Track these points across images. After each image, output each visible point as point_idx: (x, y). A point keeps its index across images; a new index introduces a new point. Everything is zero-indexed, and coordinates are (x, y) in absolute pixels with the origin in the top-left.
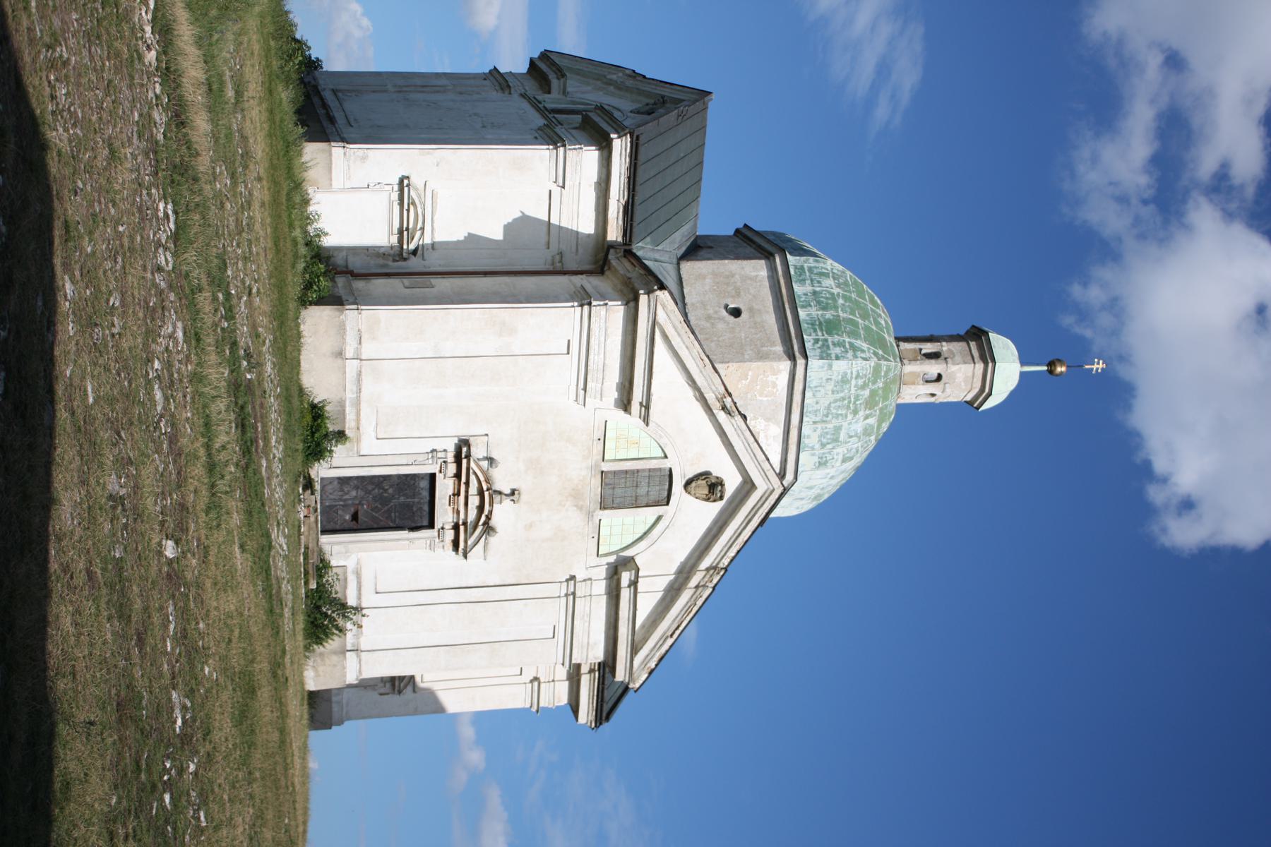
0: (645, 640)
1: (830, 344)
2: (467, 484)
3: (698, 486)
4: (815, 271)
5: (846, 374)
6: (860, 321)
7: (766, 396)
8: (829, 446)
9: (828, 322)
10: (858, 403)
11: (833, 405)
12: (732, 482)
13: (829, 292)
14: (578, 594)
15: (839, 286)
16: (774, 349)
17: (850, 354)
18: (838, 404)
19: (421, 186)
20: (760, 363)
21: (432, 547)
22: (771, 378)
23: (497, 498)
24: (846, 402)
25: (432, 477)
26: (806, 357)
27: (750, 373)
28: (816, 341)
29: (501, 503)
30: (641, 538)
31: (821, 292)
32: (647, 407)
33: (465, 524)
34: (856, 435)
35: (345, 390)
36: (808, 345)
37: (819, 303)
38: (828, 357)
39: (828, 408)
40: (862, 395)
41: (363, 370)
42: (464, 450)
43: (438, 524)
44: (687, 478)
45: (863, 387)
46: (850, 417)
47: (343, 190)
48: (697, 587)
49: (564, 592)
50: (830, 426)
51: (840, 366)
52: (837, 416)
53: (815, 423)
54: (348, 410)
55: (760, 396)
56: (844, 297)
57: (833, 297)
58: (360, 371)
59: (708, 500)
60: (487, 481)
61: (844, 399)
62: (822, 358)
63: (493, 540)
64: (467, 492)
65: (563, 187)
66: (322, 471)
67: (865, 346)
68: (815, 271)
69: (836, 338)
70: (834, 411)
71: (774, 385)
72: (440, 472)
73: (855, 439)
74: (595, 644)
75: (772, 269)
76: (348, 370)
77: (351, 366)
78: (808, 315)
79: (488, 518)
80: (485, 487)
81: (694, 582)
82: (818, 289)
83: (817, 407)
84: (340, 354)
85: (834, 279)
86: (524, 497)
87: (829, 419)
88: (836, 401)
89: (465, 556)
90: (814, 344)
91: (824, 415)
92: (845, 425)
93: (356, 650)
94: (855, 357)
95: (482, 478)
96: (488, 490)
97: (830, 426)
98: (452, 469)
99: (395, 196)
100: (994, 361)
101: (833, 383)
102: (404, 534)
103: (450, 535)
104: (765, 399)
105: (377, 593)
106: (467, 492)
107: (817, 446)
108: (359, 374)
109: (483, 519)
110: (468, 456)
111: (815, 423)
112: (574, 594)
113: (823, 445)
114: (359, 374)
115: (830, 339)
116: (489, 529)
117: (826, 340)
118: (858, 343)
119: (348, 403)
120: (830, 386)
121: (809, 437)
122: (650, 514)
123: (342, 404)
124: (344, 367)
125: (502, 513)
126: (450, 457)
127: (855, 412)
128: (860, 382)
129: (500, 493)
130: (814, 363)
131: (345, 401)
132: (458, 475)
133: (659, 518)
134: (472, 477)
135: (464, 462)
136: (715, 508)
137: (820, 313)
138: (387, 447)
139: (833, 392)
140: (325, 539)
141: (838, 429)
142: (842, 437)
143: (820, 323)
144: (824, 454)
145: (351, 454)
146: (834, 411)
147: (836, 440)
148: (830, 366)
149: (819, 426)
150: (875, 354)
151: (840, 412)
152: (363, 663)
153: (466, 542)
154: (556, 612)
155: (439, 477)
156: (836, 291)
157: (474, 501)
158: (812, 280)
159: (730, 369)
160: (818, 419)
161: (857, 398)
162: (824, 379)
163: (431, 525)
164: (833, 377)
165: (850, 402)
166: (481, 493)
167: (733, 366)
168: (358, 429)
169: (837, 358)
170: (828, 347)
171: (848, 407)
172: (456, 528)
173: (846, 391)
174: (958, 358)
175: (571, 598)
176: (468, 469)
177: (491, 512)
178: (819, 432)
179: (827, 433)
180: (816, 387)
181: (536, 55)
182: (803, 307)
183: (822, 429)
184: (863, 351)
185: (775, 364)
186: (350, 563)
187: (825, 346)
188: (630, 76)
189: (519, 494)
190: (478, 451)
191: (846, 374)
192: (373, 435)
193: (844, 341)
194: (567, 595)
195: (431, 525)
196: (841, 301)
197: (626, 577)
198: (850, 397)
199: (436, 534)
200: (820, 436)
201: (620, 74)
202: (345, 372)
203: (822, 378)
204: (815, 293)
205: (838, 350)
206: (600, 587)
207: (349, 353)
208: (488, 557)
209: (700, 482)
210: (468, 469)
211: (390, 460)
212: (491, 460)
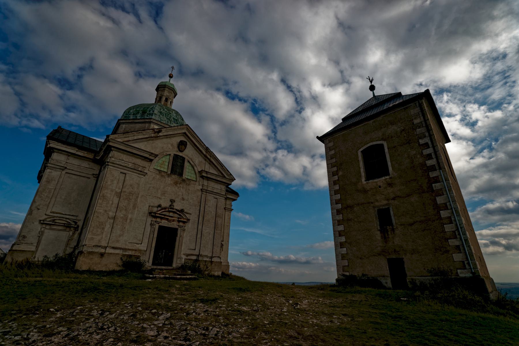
0: (222, 174)
2: (165, 215)
3: (181, 148)
4: (127, 113)
5: (159, 111)
8: (178, 122)
9: (143, 112)
12: (183, 139)
14: (206, 189)
16: (146, 127)
17: (153, 109)
19: (47, 217)
21: (184, 230)
23: (172, 207)
25: (159, 226)
26: (151, 119)
28: (147, 116)
29: (174, 206)
30: (194, 168)
32: (152, 154)
33: (178, 218)
35: (119, 254)
36: (148, 118)
37: (136, 114)
38: (152, 114)
39: (167, 119)
41: (112, 246)
42: (152, 214)
43: (177, 227)
44: (178, 150)
46: (171, 115)
47: (37, 247)
48: (210, 156)
49: (205, 193)
50: (172, 120)
51: (156, 112)
53: (171, 123)
54: (127, 253)
57: (136, 111)
58: (112, 247)
59: (186, 147)
60: (165, 208)
61: (166, 115)
62: (152, 115)
63: (185, 211)
64: (167, 216)
65: (66, 168)
66: (149, 265)
72: (159, 224)
73: (177, 116)
75: (123, 123)
76: (110, 252)
77: (109, 250)
79: (178, 211)
80: (167, 210)
81: (209, 157)
84: (102, 255)
86: (173, 198)
88: (166, 116)
89: (189, 220)
92: (173, 116)
93: (212, 257)
94: (155, 108)
95: (164, 210)
96: (168, 209)
97: (172, 120)
98: (158, 220)
99: (48, 227)
100: (165, 85)
102: (178, 238)
103: (181, 224)
105: (195, 249)
106: (167, 216)
108: (114, 248)
109: (178, 212)
110: (155, 213)
111: (171, 123)
112: (206, 190)
113: (177, 123)
114: (114, 248)
115: (148, 113)
116: (182, 211)
117: (148, 114)
119: (124, 253)
120: (161, 116)
122: (186, 164)
123: (124, 255)
124: (108, 253)
125: (177, 206)
126: (154, 220)
127: (170, 114)
129: (170, 205)
130: (153, 117)
131: (123, 254)
132: (162, 218)
133: (188, 161)
134: (163, 213)
135: (157, 215)
136: (189, 145)
137: (139, 114)
138: (146, 241)
140: (174, 265)
141: (174, 118)
142: (176, 118)
145: (145, 254)
147: (177, 120)
148: (155, 114)
152: (216, 256)
153: (184, 219)
154: (210, 197)
155: (160, 224)
157: (171, 214)
158: (130, 115)
160: (170, 122)
161: (166, 111)
163: (176, 230)
166: (169, 212)
168: (136, 250)
169: (153, 112)
172: (179, 221)
174: (163, 93)
175: (207, 191)
176: (160, 214)
177: (176, 210)
178: (173, 123)
182: (137, 117)
186: (184, 257)
187: (150, 114)
189: (172, 200)
190: (155, 210)
191: (159, 111)
192: (139, 245)
194: (206, 192)
195: (176, 230)
197: (204, 174)
199: (180, 228)
200: (175, 122)
202: (111, 253)
204: (133, 115)
205: (151, 111)
206: (206, 183)
207: (103, 251)
208: (191, 213)
209: (180, 147)
210: (160, 214)
211: (151, 240)
212: (159, 206)
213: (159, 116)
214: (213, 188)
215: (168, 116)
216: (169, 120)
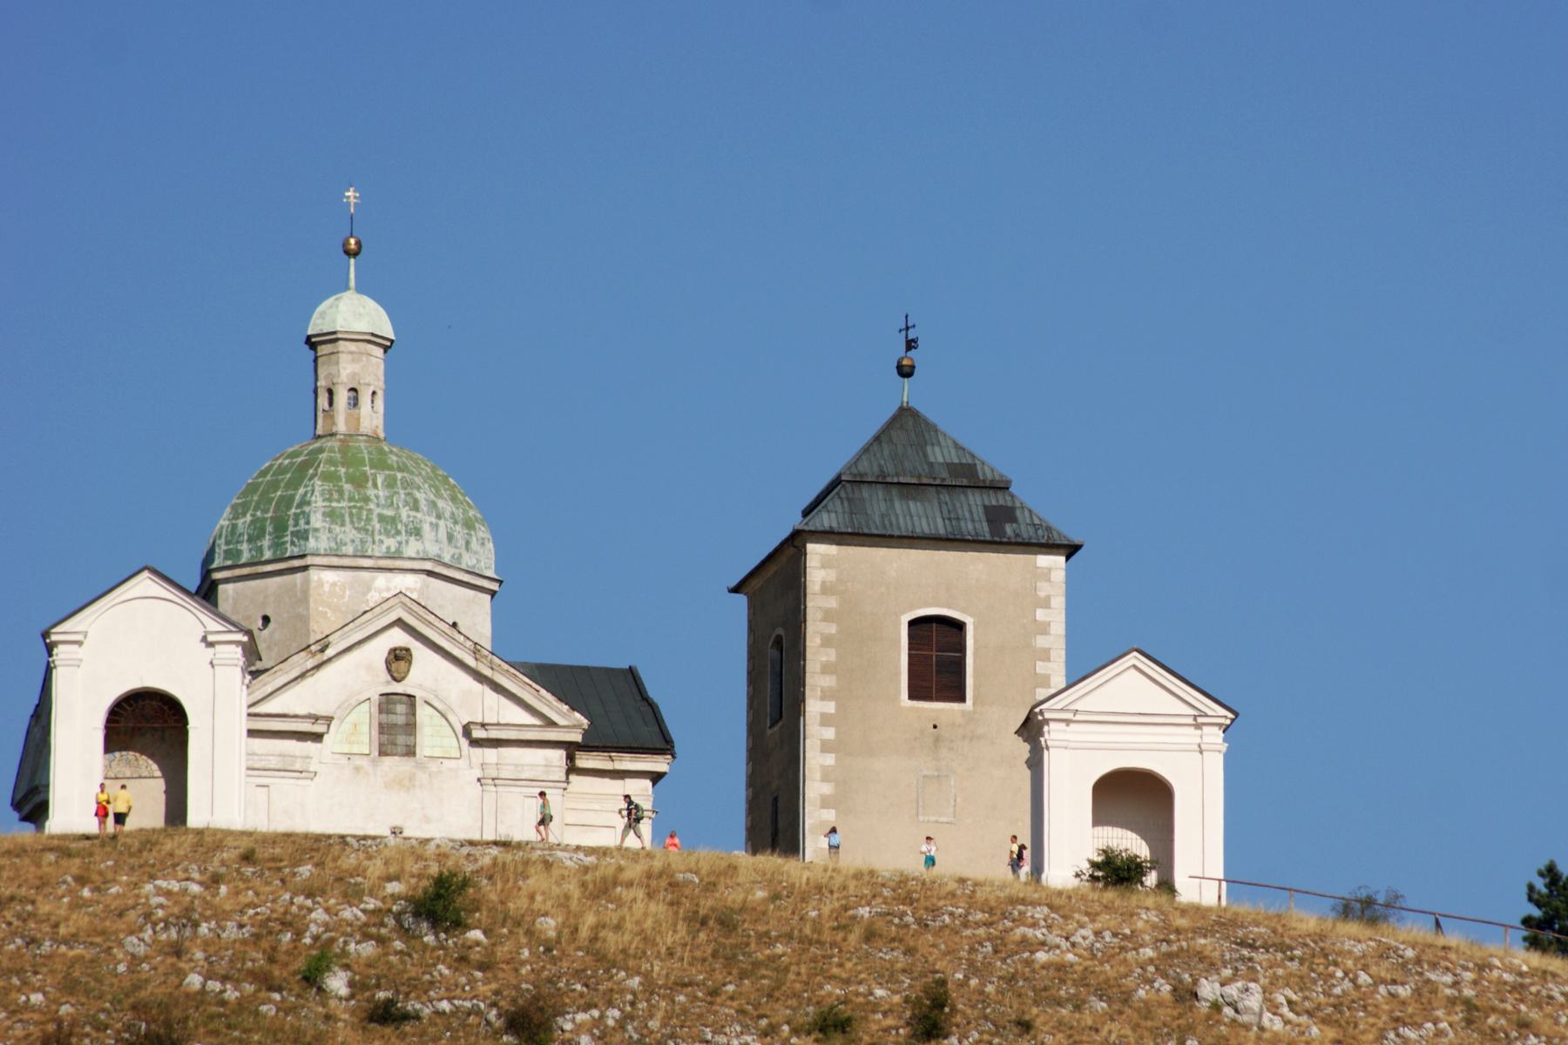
1: (296, 529)
6: (279, 493)
7: (344, 592)
8: (399, 527)
10: (357, 497)
11: (356, 525)
13: (249, 526)
15: (244, 515)
16: (299, 585)
18: (355, 520)
20: (311, 600)
22: (326, 588)
24: (354, 511)
27: (321, 609)
31: (249, 535)
34: (391, 497)
40: (350, 491)
45: (341, 492)
52: (368, 520)
53: (374, 543)
55: (343, 597)
56: (256, 509)
61: (351, 515)
67: (301, 491)
68: (229, 538)
69: (291, 522)
70: (363, 523)
71: (334, 584)
74: (546, 760)
78: (269, 549)
82: (246, 537)
83: (358, 542)
85: (237, 518)
87: (370, 528)
88: (352, 522)
90: (295, 546)
91: (367, 534)
92: (378, 511)
97: (378, 526)
101: (333, 527)
104: (348, 593)
107: (399, 538)
111: (374, 543)
112: (493, 779)
117: (292, 533)
118: (297, 498)
120: (337, 529)
121: (388, 548)
128: (336, 496)
139: (343, 525)
141: (381, 518)
142: (389, 513)
143: (277, 537)
144: (406, 531)
146: (363, 523)
147: (393, 520)
149: (377, 538)
150: (310, 479)
151: (364, 517)
156: (249, 518)
159: (315, 628)
160: (370, 539)
161: (351, 499)
162: (329, 535)
164: (327, 526)
165: (355, 507)
167: (313, 626)
170: (299, 531)
171: (361, 508)
173: (343, 511)
178: (383, 537)
179: (385, 529)
180: (336, 543)
181: (15, 815)
183: (380, 533)
184: (306, 493)
185: (313, 585)
188: (37, 722)
193: (295, 514)
196: (259, 513)
198: (350, 507)
200: (388, 534)
201: (36, 730)
203: (328, 539)
206: (491, 754)
213: (330, 531)
214: (516, 765)
215: (360, 519)
216: (367, 530)
